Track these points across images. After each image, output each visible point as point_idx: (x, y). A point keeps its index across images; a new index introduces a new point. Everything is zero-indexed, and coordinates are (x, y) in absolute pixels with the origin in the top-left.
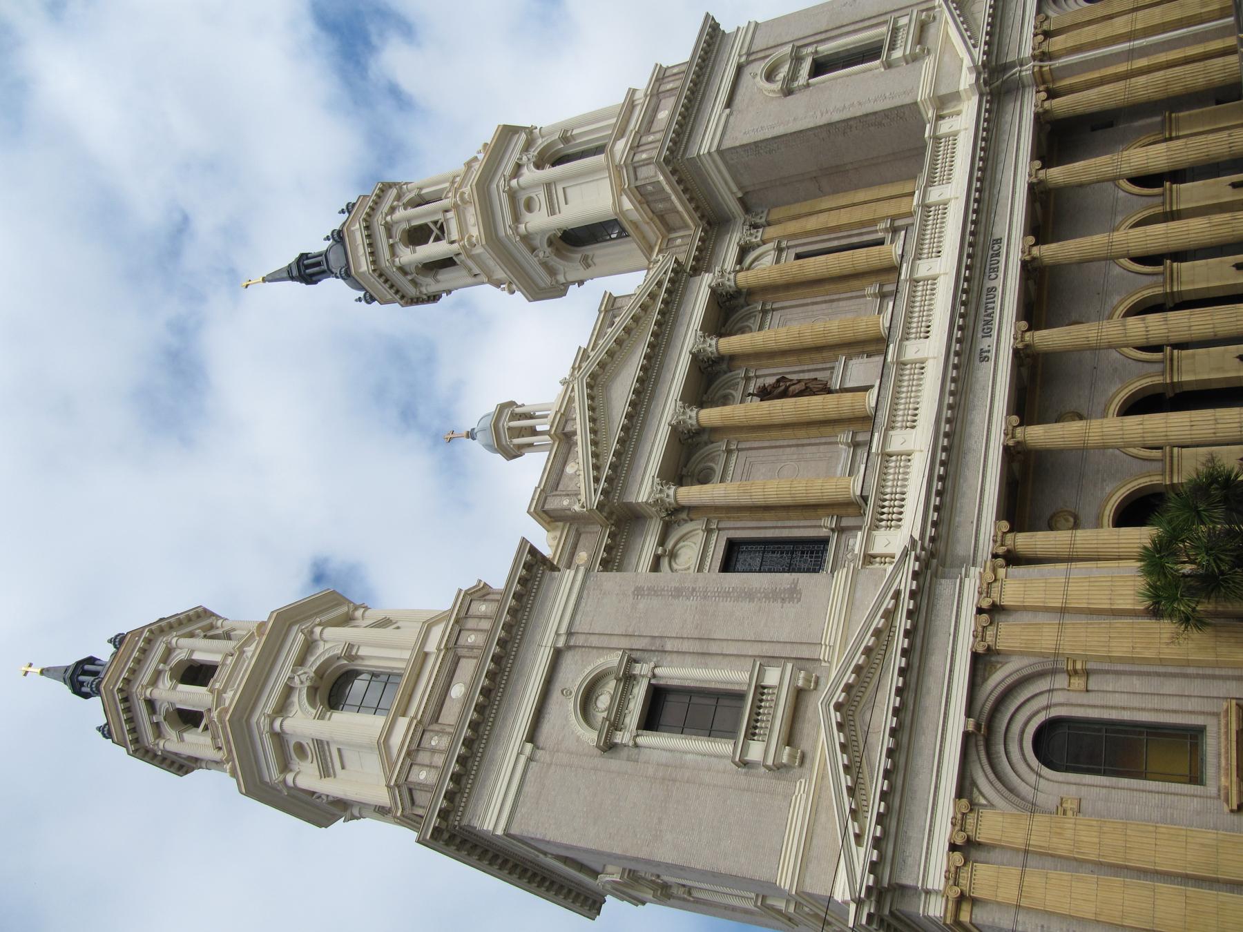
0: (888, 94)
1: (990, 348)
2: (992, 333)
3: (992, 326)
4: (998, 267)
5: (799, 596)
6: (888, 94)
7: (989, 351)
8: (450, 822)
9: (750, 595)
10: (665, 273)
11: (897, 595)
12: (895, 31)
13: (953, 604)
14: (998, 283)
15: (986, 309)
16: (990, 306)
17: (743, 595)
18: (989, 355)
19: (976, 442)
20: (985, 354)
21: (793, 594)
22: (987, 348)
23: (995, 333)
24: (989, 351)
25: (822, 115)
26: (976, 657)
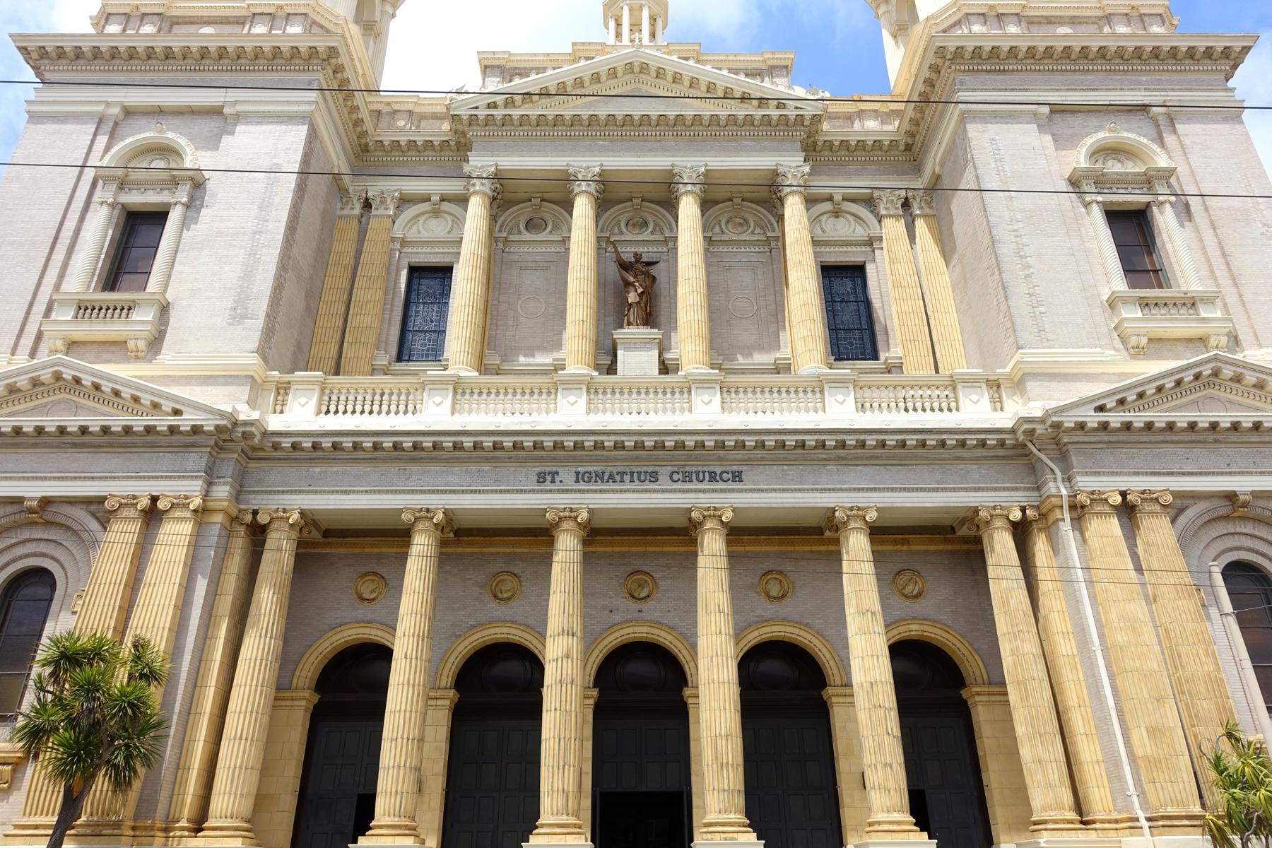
0: (1042, 309)
1: (558, 483)
2: (582, 483)
3: (592, 483)
4: (691, 481)
5: (236, 323)
6: (1042, 309)
7: (553, 481)
8: (41, 62)
9: (247, 275)
10: (796, 108)
11: (177, 412)
12: (1191, 303)
13: (175, 471)
14: (664, 482)
15: (622, 474)
16: (627, 478)
17: (249, 269)
18: (548, 483)
19: (418, 479)
20: (549, 478)
21: (238, 315)
22: (557, 478)
23: (582, 486)
24: (553, 481)
25: (1015, 231)
26: (101, 500)
